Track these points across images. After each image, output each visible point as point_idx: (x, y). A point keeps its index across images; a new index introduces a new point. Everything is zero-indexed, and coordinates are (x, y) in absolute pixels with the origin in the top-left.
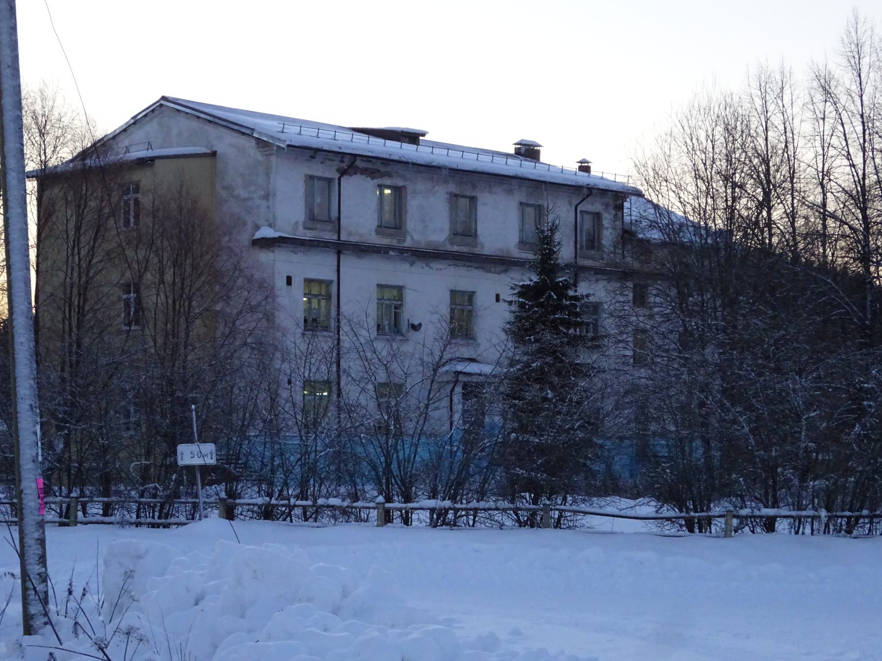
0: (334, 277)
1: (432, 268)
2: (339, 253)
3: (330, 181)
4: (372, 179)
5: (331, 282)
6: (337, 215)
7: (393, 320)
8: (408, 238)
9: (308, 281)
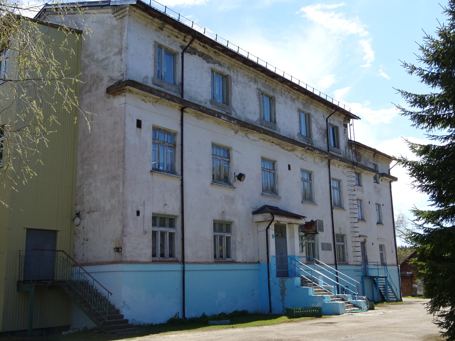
1: (249, 138)
2: (182, 110)
3: (172, 54)
4: (208, 62)
8: (233, 113)
9: (156, 129)
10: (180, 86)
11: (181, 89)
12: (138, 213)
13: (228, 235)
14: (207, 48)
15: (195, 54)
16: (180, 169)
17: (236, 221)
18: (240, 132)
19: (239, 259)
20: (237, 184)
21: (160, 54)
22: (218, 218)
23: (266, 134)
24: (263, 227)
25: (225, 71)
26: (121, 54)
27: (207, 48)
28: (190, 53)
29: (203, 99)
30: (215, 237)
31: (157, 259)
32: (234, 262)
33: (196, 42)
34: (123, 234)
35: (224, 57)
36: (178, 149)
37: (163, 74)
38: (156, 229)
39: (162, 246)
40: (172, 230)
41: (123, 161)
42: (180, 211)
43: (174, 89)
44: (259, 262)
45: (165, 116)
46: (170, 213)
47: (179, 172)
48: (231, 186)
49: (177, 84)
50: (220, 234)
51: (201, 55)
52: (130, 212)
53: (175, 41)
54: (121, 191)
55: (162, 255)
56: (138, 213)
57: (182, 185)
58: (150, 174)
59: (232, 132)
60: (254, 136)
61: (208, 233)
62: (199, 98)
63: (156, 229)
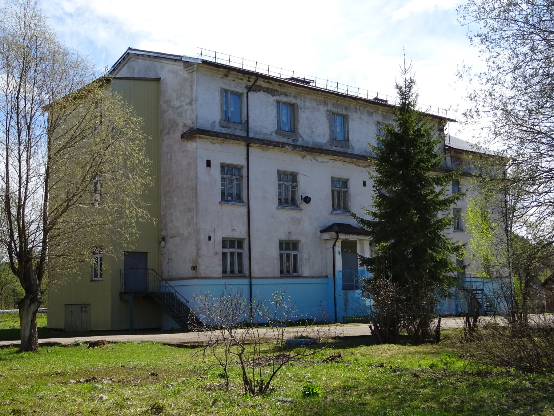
0: (244, 163)
3: (240, 95)
4: (273, 96)
5: (242, 167)
6: (246, 119)
7: (290, 196)
8: (300, 139)
10: (246, 123)
11: (246, 126)
12: (210, 238)
13: (295, 253)
14: (271, 83)
15: (260, 91)
16: (246, 198)
17: (303, 240)
18: (307, 157)
19: (306, 274)
20: (304, 206)
21: (226, 97)
22: (284, 237)
23: (335, 155)
24: (331, 243)
25: (291, 100)
26: (192, 105)
27: (271, 83)
28: (255, 91)
29: (268, 132)
30: (281, 256)
31: (227, 275)
32: (300, 277)
33: (260, 80)
34: (198, 256)
35: (289, 87)
36: (245, 180)
37: (230, 116)
38: (225, 250)
39: (232, 264)
40: (240, 251)
41: (196, 196)
42: (247, 234)
43: (240, 127)
44: (327, 276)
45: (233, 154)
46: (238, 237)
47: (246, 201)
48: (298, 209)
49: (243, 121)
50: (287, 252)
51: (266, 90)
52: (203, 237)
53: (240, 83)
54: (195, 221)
55: (232, 272)
56: (210, 238)
57: (249, 212)
58: (219, 205)
59: (299, 158)
60: (322, 158)
61: (274, 252)
62: (265, 131)
63: (225, 250)
